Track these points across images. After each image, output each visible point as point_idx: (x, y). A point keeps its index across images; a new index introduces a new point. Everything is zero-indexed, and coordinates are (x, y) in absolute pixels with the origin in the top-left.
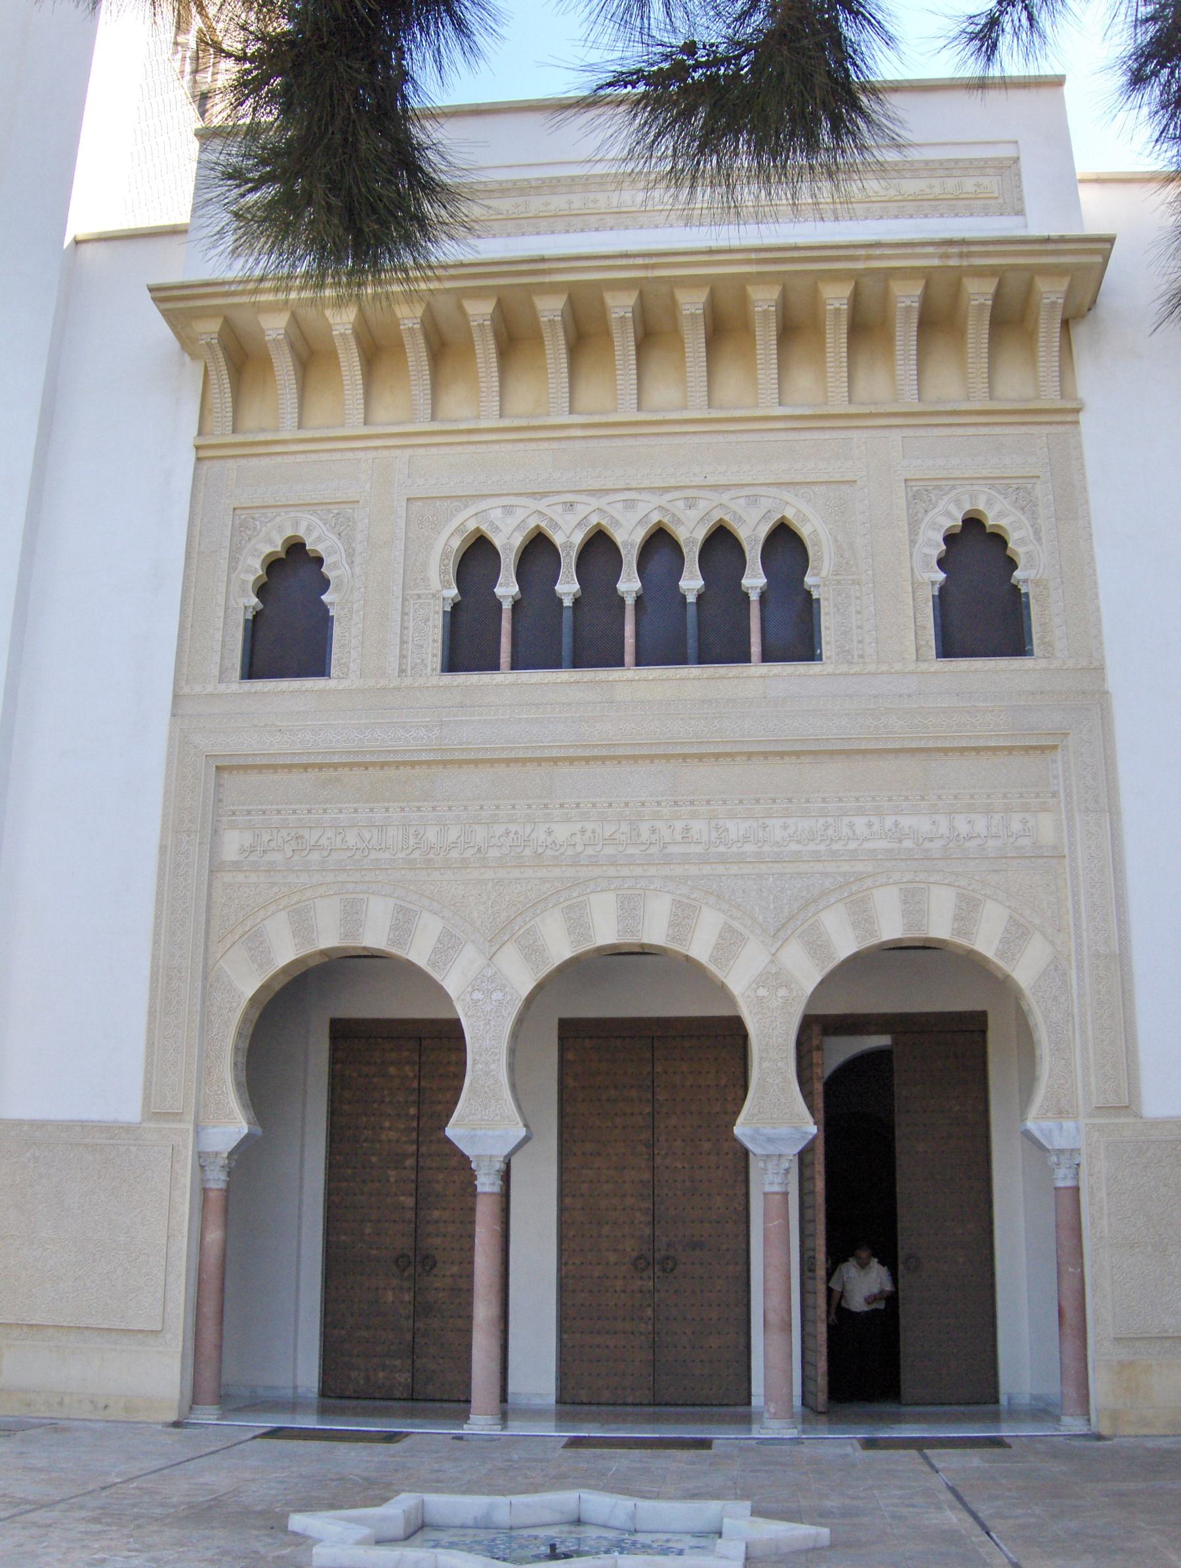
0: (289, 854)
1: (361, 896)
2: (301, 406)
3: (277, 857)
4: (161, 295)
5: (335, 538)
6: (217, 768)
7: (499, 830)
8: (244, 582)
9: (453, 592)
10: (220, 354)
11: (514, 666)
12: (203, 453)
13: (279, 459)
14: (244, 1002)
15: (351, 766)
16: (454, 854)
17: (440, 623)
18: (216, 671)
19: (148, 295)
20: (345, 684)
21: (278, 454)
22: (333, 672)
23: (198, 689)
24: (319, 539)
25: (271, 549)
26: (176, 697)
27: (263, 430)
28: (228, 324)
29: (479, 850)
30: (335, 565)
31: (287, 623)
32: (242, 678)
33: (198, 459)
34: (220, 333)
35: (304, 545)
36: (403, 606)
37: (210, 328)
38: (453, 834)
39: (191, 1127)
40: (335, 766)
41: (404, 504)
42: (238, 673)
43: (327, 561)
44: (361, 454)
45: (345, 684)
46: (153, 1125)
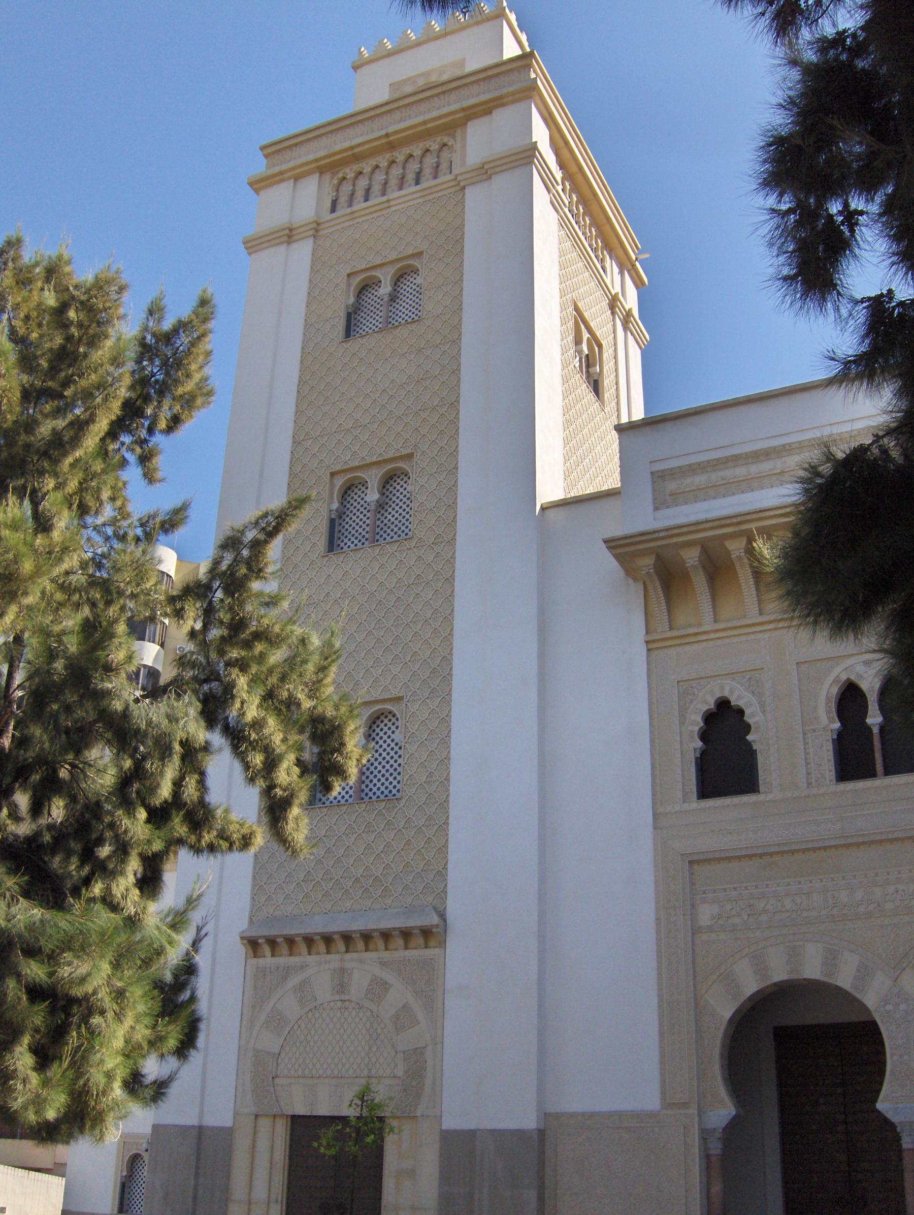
0: (746, 918)
1: (798, 943)
2: (714, 607)
3: (737, 920)
4: (612, 544)
5: (751, 696)
6: (689, 862)
7: (891, 889)
8: (692, 731)
9: (837, 725)
10: (655, 578)
11: (887, 772)
12: (651, 646)
13: (704, 644)
14: (725, 1023)
15: (782, 853)
16: (862, 909)
17: (830, 747)
18: (680, 795)
19: (604, 546)
20: (770, 797)
21: (703, 641)
22: (761, 789)
23: (669, 808)
24: (739, 697)
25: (708, 707)
26: (655, 815)
27: (690, 626)
28: (659, 558)
29: (879, 905)
30: (753, 715)
31: (724, 757)
32: (698, 799)
33: (648, 650)
34: (654, 565)
35: (729, 702)
36: (804, 738)
37: (648, 562)
38: (859, 895)
39: (696, 1112)
40: (771, 854)
41: (795, 667)
42: (695, 795)
43: (747, 712)
44: (759, 636)
45: (770, 797)
46: (669, 1112)
